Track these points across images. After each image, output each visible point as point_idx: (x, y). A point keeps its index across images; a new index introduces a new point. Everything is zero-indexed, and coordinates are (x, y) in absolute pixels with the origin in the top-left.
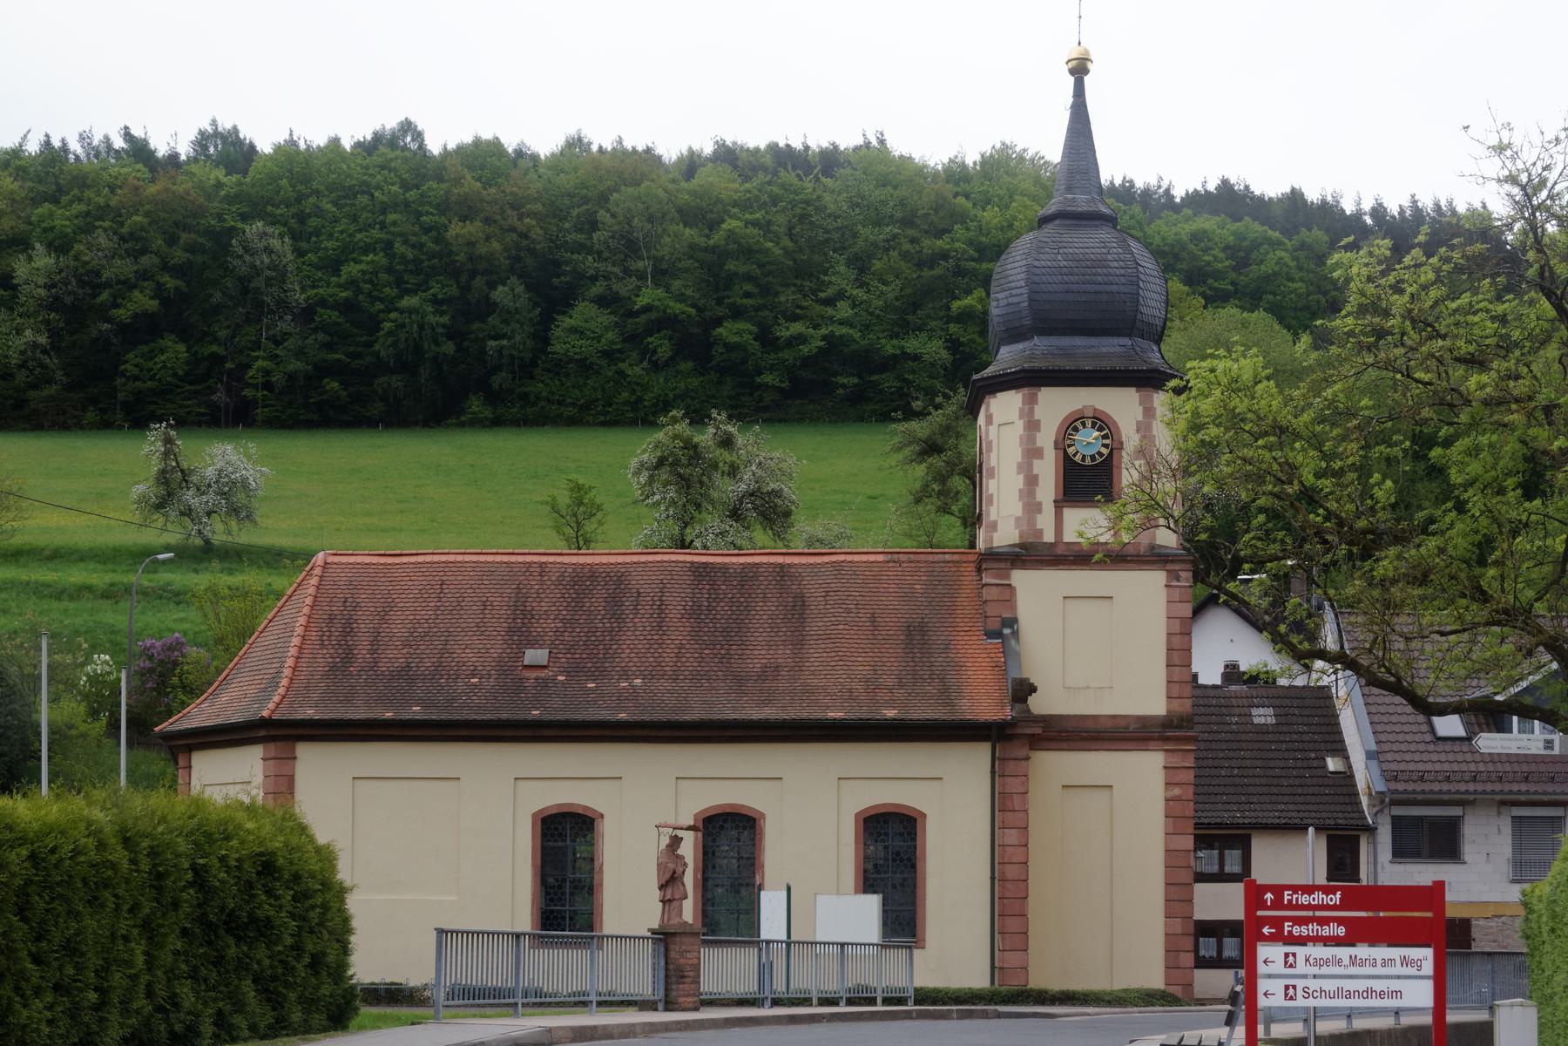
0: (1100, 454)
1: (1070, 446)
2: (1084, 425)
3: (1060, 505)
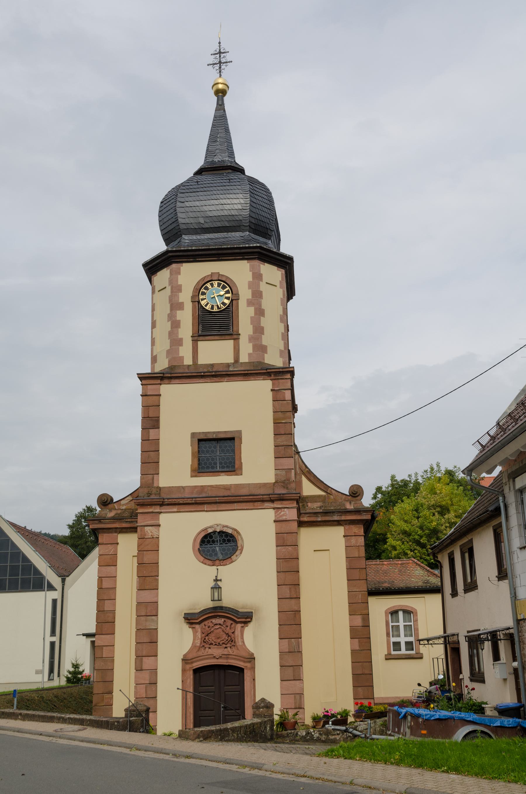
1: (202, 300)
2: (212, 285)
3: (196, 338)
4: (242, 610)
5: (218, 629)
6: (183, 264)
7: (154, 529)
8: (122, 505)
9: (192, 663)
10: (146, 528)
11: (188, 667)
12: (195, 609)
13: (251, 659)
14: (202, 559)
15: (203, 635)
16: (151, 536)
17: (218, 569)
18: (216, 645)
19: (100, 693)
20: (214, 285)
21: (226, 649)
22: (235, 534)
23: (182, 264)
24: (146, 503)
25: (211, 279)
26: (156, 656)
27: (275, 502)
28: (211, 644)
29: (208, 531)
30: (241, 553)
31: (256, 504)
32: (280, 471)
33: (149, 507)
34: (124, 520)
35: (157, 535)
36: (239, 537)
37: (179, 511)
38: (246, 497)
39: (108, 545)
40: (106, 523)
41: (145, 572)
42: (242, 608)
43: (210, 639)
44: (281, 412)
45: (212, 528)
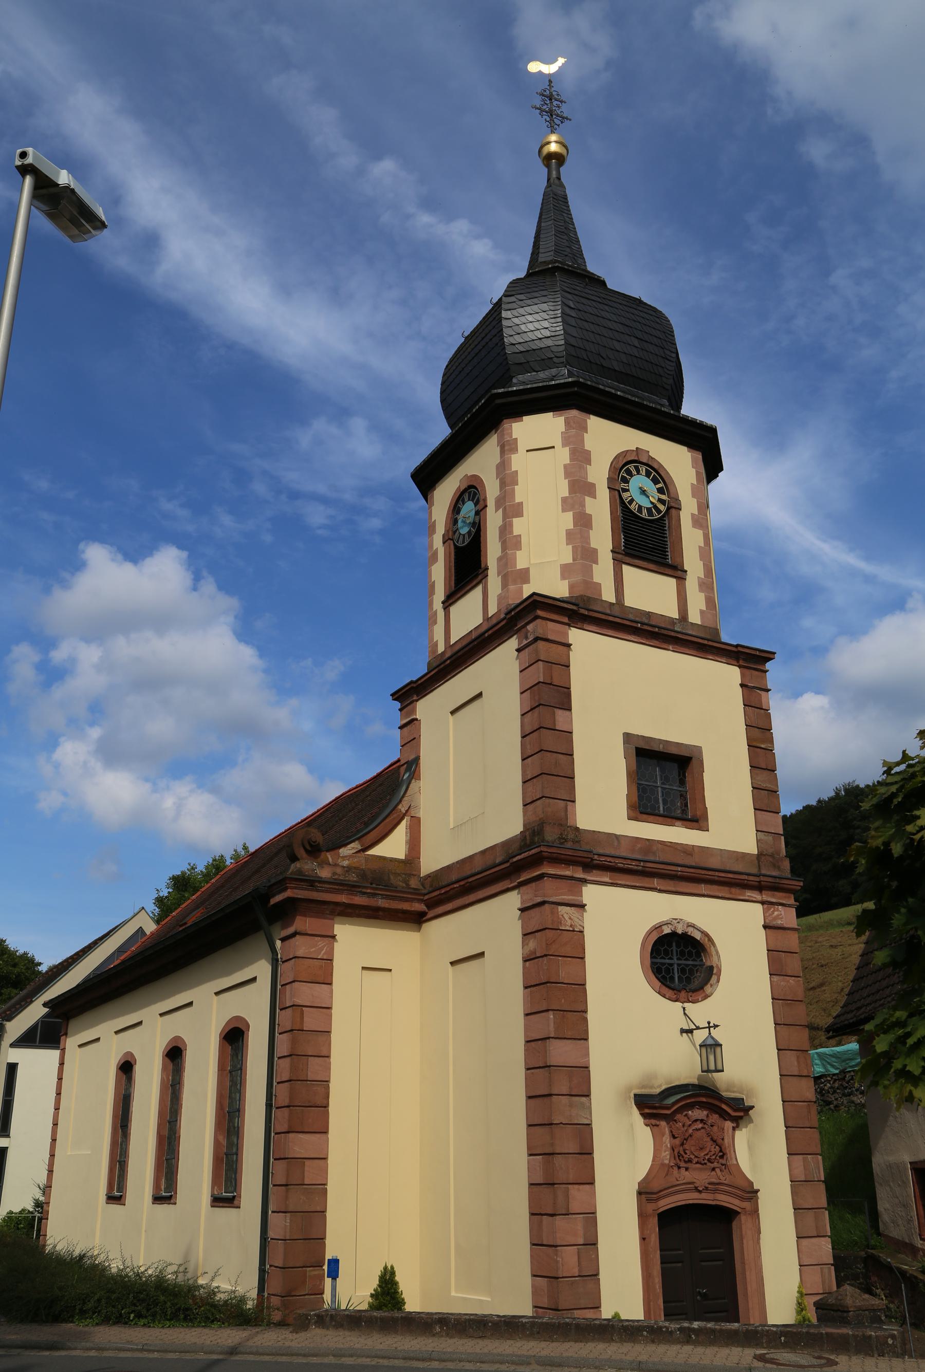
0: (659, 511)
3: (620, 556)
4: (726, 1093)
5: (699, 1129)
6: (524, 417)
7: (575, 912)
8: (342, 857)
9: (658, 1199)
10: (560, 908)
11: (650, 1207)
12: (652, 1087)
13: (751, 1193)
14: (658, 984)
15: (677, 1141)
16: (571, 926)
17: (684, 1009)
18: (697, 1163)
19: (298, 1266)
20: (641, 471)
21: (713, 1173)
22: (705, 941)
23: (588, 415)
24: (563, 856)
25: (636, 459)
26: (592, 1183)
27: (763, 892)
28: (690, 1161)
29: (663, 931)
30: (718, 981)
31: (733, 890)
32: (765, 835)
33: (563, 865)
34: (360, 890)
35: (581, 926)
36: (712, 947)
37: (615, 882)
38: (723, 875)
39: (316, 938)
40: (322, 891)
41: (563, 1001)
42: (727, 1091)
43: (687, 1151)
44: (758, 728)
45: (669, 925)
